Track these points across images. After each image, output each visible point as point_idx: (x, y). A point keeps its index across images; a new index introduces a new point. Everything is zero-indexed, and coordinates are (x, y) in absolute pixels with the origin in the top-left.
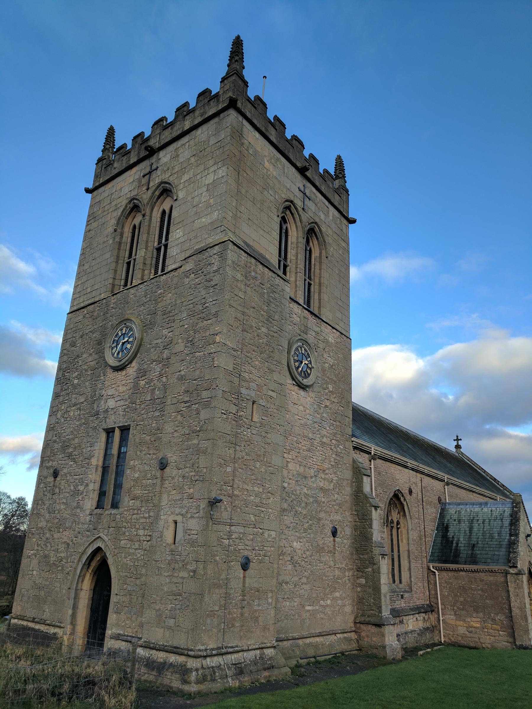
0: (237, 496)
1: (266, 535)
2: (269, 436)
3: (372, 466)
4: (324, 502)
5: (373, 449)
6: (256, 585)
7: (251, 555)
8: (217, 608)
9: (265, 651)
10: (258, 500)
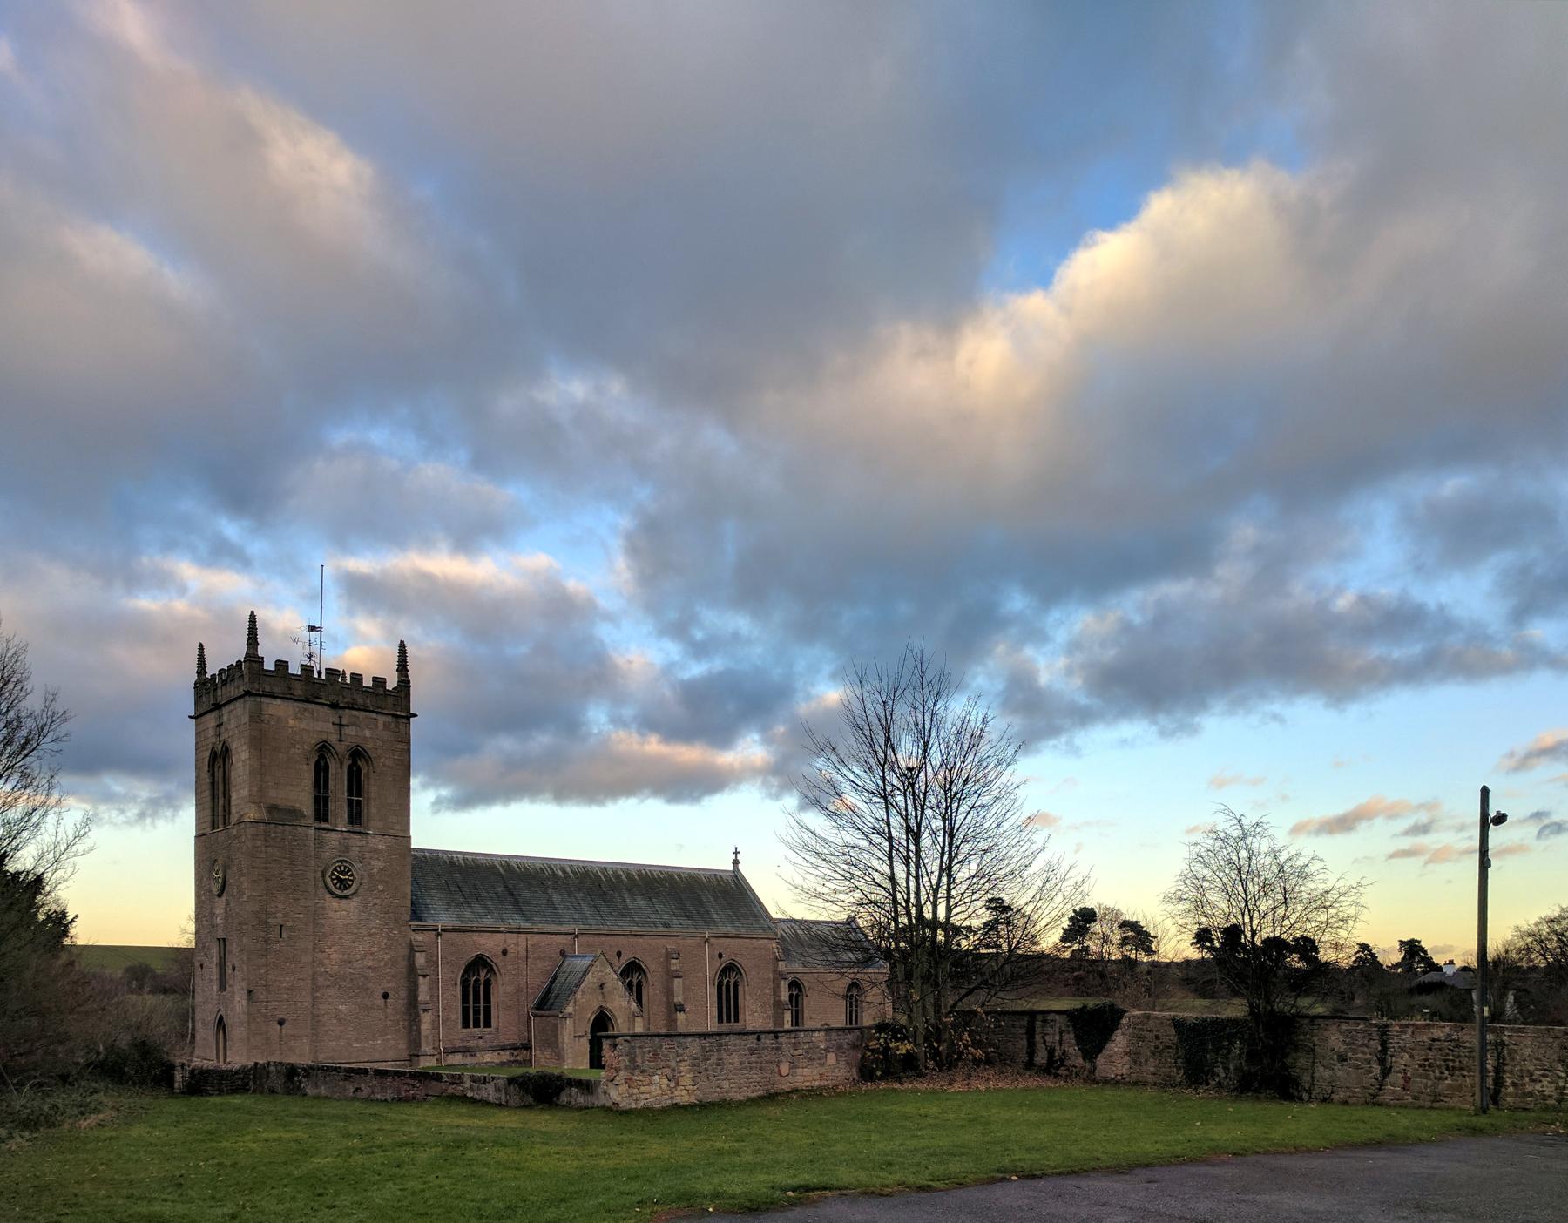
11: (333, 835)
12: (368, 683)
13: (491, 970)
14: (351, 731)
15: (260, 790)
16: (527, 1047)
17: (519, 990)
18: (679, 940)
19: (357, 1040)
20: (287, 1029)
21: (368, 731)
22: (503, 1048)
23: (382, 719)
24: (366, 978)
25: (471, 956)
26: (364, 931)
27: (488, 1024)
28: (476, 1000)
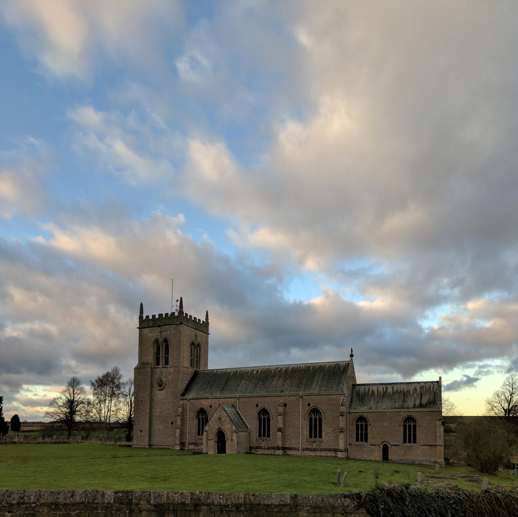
11: (158, 369)
14: (164, 333)
18: (286, 398)
23: (173, 326)
25: (199, 407)
26: (166, 401)
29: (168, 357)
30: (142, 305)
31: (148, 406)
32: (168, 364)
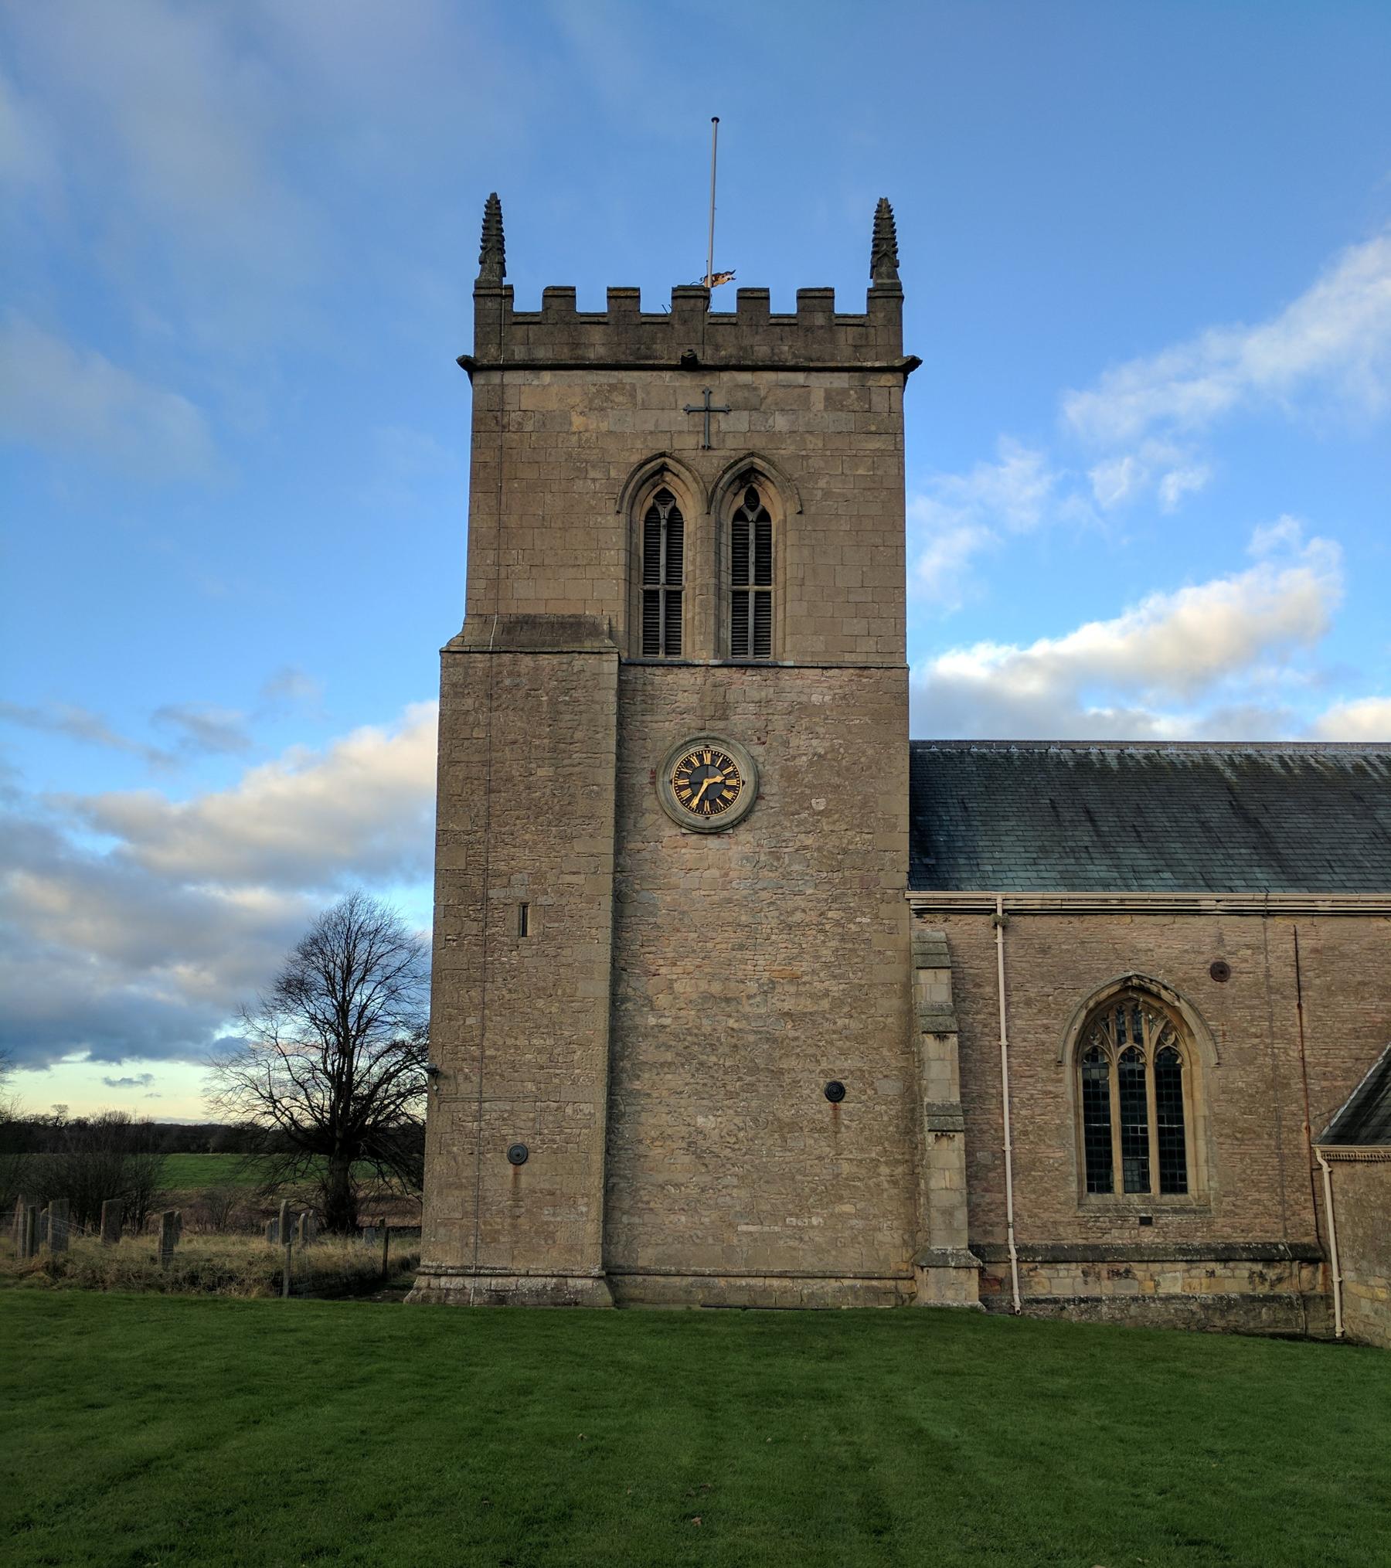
0: (494, 1057)
1: (569, 1110)
2: (567, 952)
3: (1000, 940)
4: (796, 1039)
5: (999, 901)
6: (547, 1186)
7: (529, 1142)
8: (458, 1215)
9: (569, 1280)
10: (543, 1059)
11: (683, 677)
12: (784, 303)
13: (1174, 1023)
15: (495, 583)
16: (1313, 1256)
17: (1276, 1083)
19: (751, 1214)
20: (533, 1175)
21: (784, 416)
22: (1226, 1255)
23: (820, 384)
24: (772, 1040)
25: (1103, 983)
26: (771, 919)
27: (1174, 1182)
28: (1133, 1109)
29: (763, 598)
30: (493, 211)
31: (602, 953)
32: (762, 643)
